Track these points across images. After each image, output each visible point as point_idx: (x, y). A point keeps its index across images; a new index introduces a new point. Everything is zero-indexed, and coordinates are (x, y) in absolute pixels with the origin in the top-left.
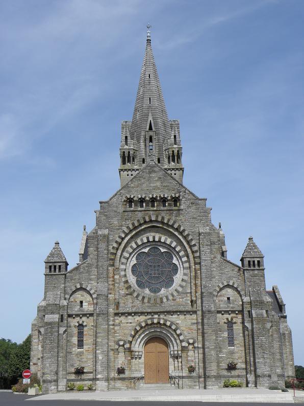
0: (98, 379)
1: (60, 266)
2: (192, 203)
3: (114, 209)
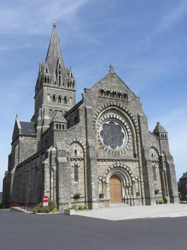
0: (94, 202)
1: (63, 125)
2: (134, 99)
3: (94, 94)
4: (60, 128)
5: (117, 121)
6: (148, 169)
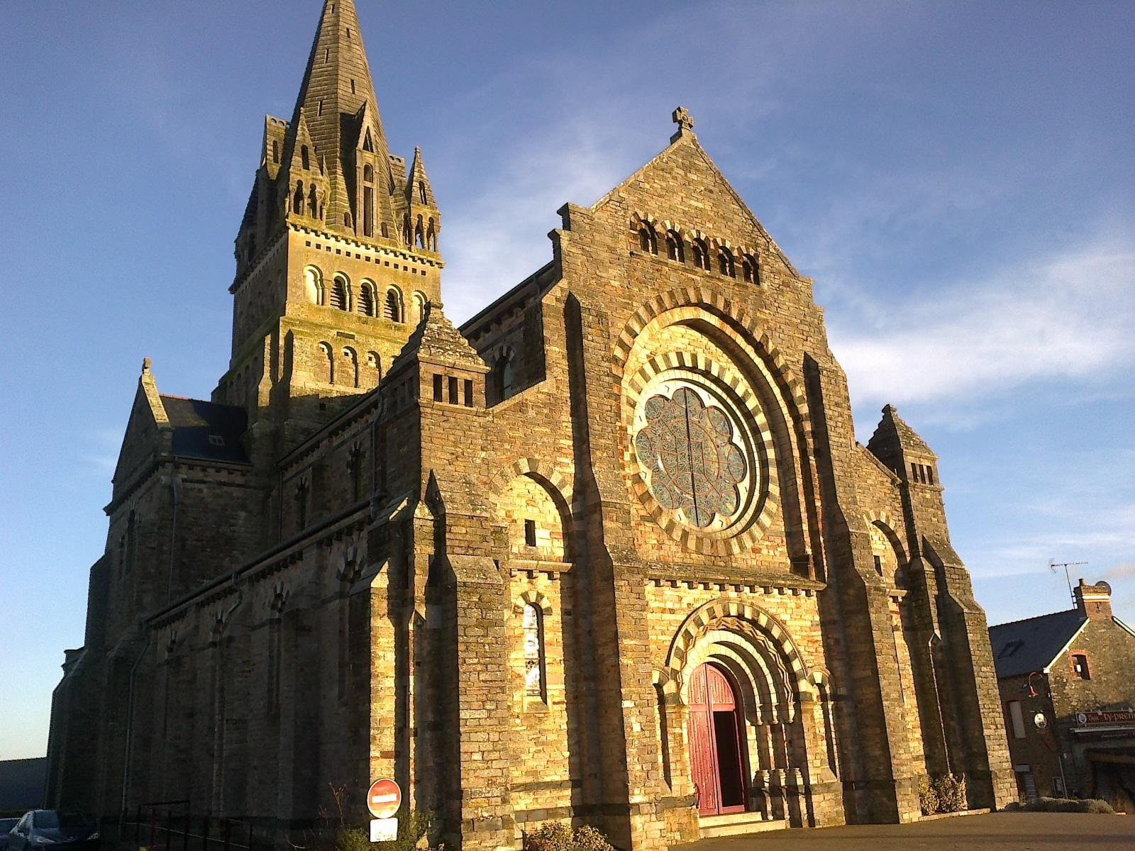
1: (468, 384)
3: (609, 241)
4: (453, 398)
5: (713, 387)
6: (876, 634)
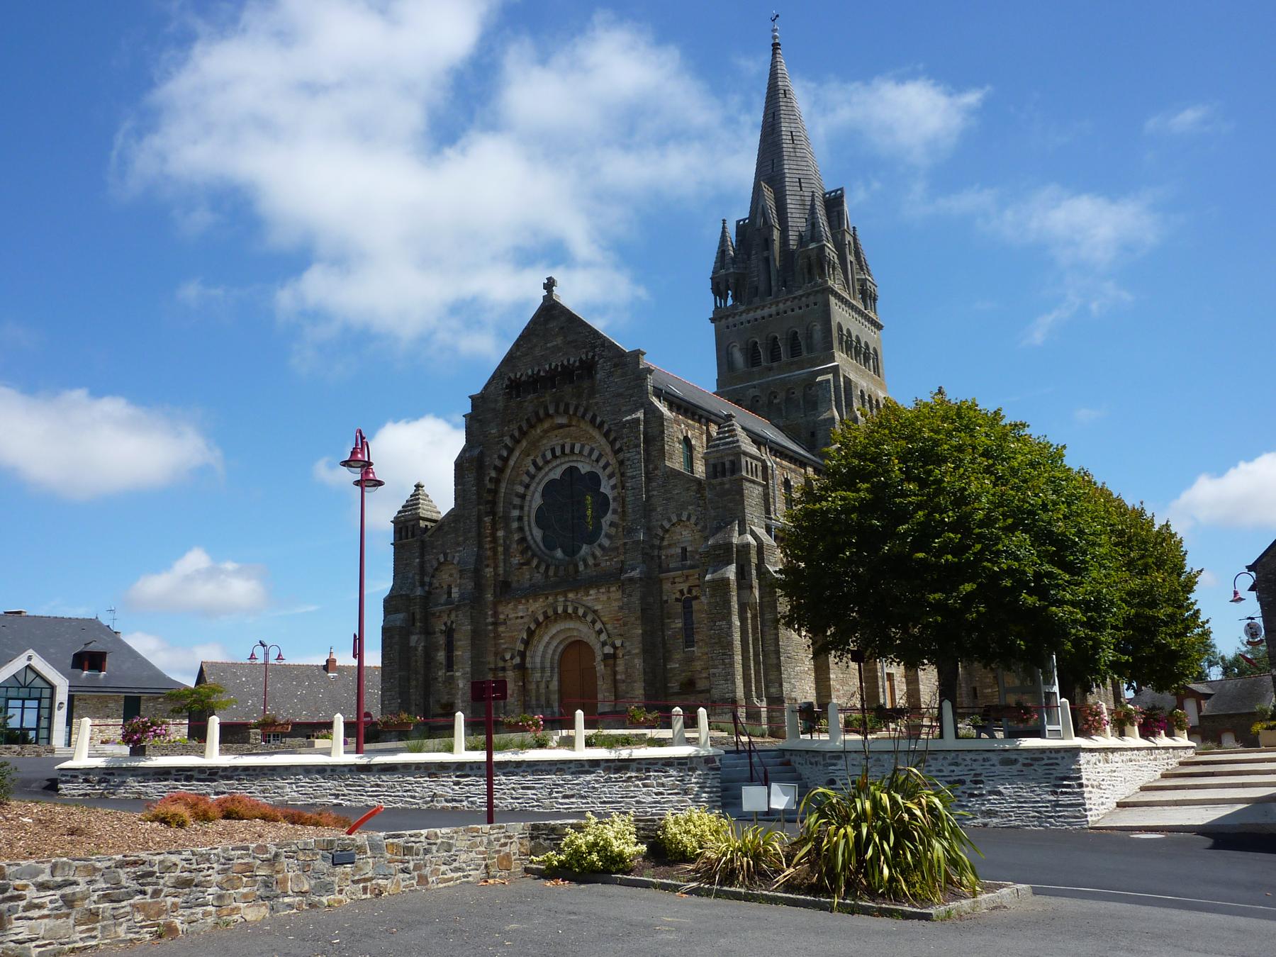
2: (616, 365)
